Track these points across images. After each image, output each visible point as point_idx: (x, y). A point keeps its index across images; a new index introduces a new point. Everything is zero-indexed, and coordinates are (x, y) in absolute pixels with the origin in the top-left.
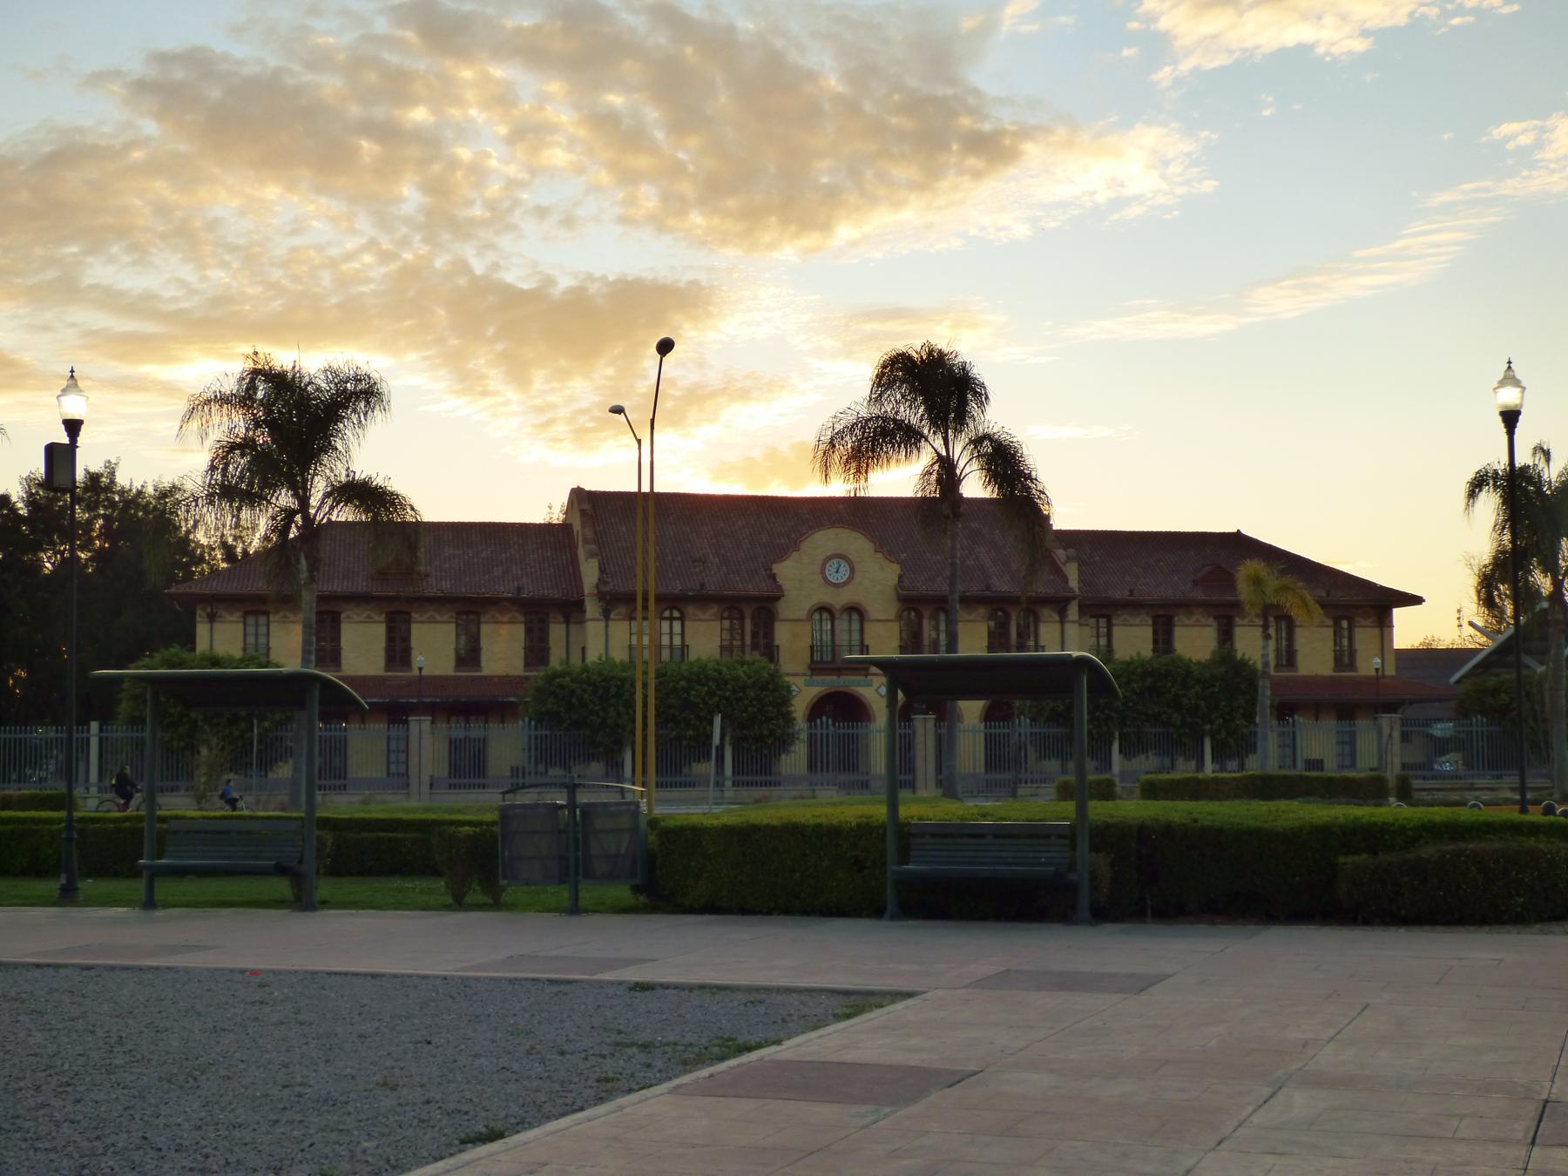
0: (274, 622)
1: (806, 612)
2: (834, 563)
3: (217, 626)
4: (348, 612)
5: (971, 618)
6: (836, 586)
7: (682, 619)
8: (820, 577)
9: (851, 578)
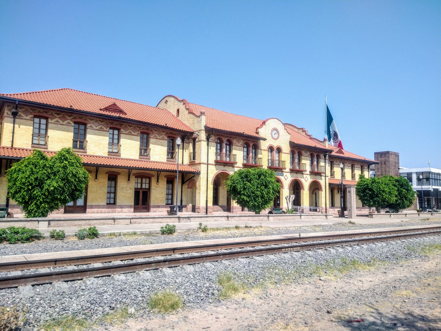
0: (51, 123)
1: (266, 148)
3: (17, 120)
4: (91, 124)
8: (270, 135)
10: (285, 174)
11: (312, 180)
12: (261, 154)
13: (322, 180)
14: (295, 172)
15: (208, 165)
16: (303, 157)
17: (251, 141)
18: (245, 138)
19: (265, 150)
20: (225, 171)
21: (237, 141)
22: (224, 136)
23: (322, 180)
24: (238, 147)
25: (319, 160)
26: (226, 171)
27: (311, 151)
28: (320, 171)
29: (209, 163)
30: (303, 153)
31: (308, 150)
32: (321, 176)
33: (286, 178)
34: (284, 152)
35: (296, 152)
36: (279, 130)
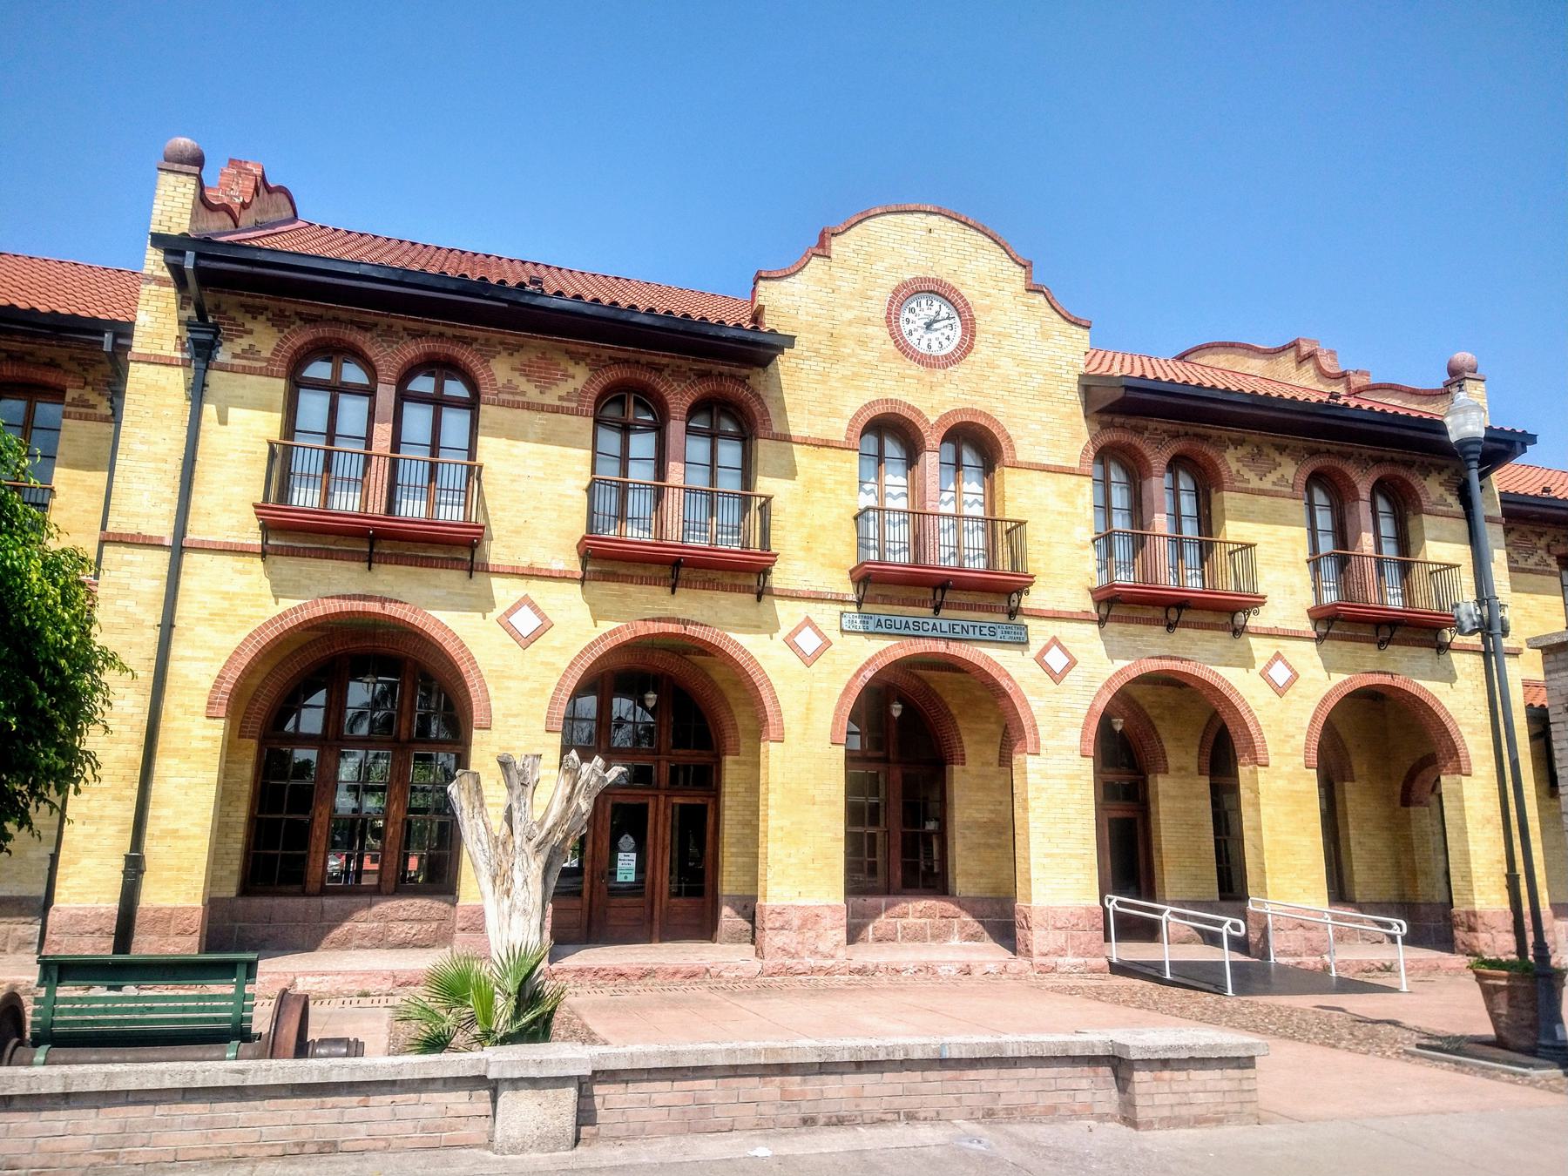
1: (843, 425)
2: (927, 308)
5: (1267, 484)
6: (929, 361)
7: (472, 405)
8: (884, 333)
9: (966, 348)
10: (1039, 632)
11: (1339, 678)
12: (790, 472)
13: (1450, 677)
14: (1158, 613)
15: (179, 549)
16: (1229, 500)
17: (678, 374)
18: (608, 350)
19: (826, 444)
20: (374, 607)
21: (526, 371)
22: (389, 333)
23: (1450, 677)
24: (538, 418)
25: (1412, 524)
26: (383, 600)
27: (1314, 453)
28: (1425, 602)
29: (197, 531)
30: (1234, 466)
31: (1281, 449)
32: (1442, 648)
33: (1056, 660)
34: (1021, 457)
35: (1158, 460)
36: (970, 293)
